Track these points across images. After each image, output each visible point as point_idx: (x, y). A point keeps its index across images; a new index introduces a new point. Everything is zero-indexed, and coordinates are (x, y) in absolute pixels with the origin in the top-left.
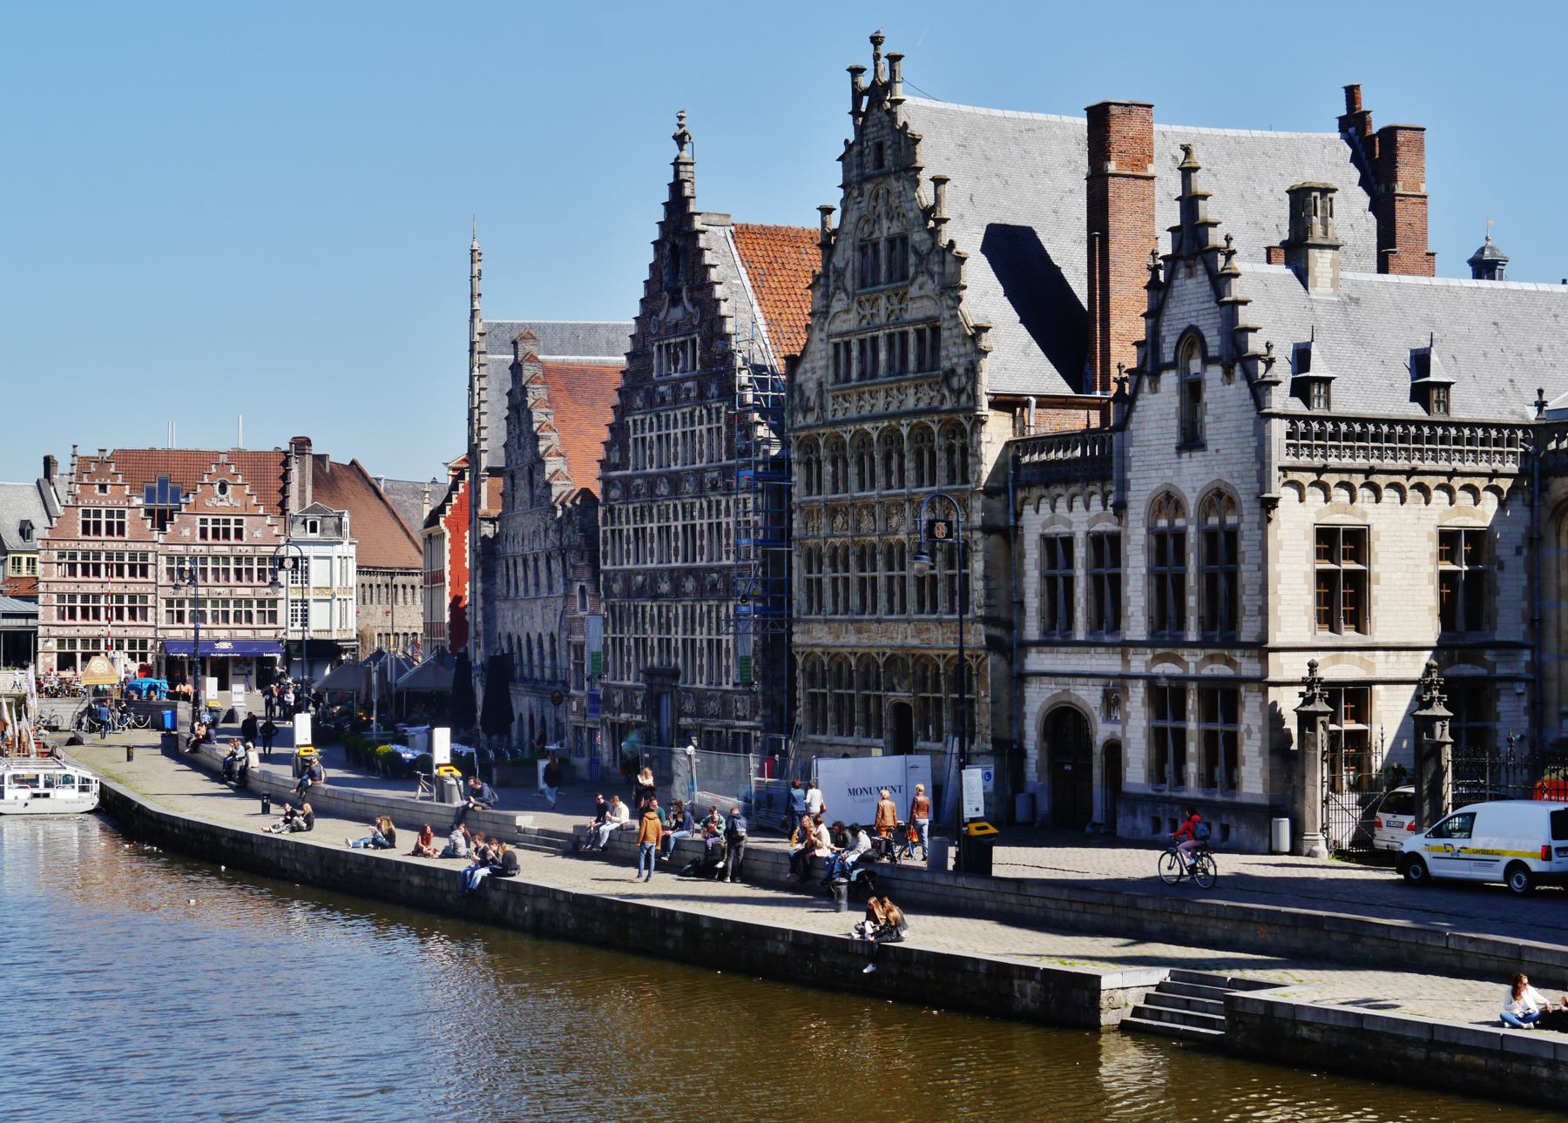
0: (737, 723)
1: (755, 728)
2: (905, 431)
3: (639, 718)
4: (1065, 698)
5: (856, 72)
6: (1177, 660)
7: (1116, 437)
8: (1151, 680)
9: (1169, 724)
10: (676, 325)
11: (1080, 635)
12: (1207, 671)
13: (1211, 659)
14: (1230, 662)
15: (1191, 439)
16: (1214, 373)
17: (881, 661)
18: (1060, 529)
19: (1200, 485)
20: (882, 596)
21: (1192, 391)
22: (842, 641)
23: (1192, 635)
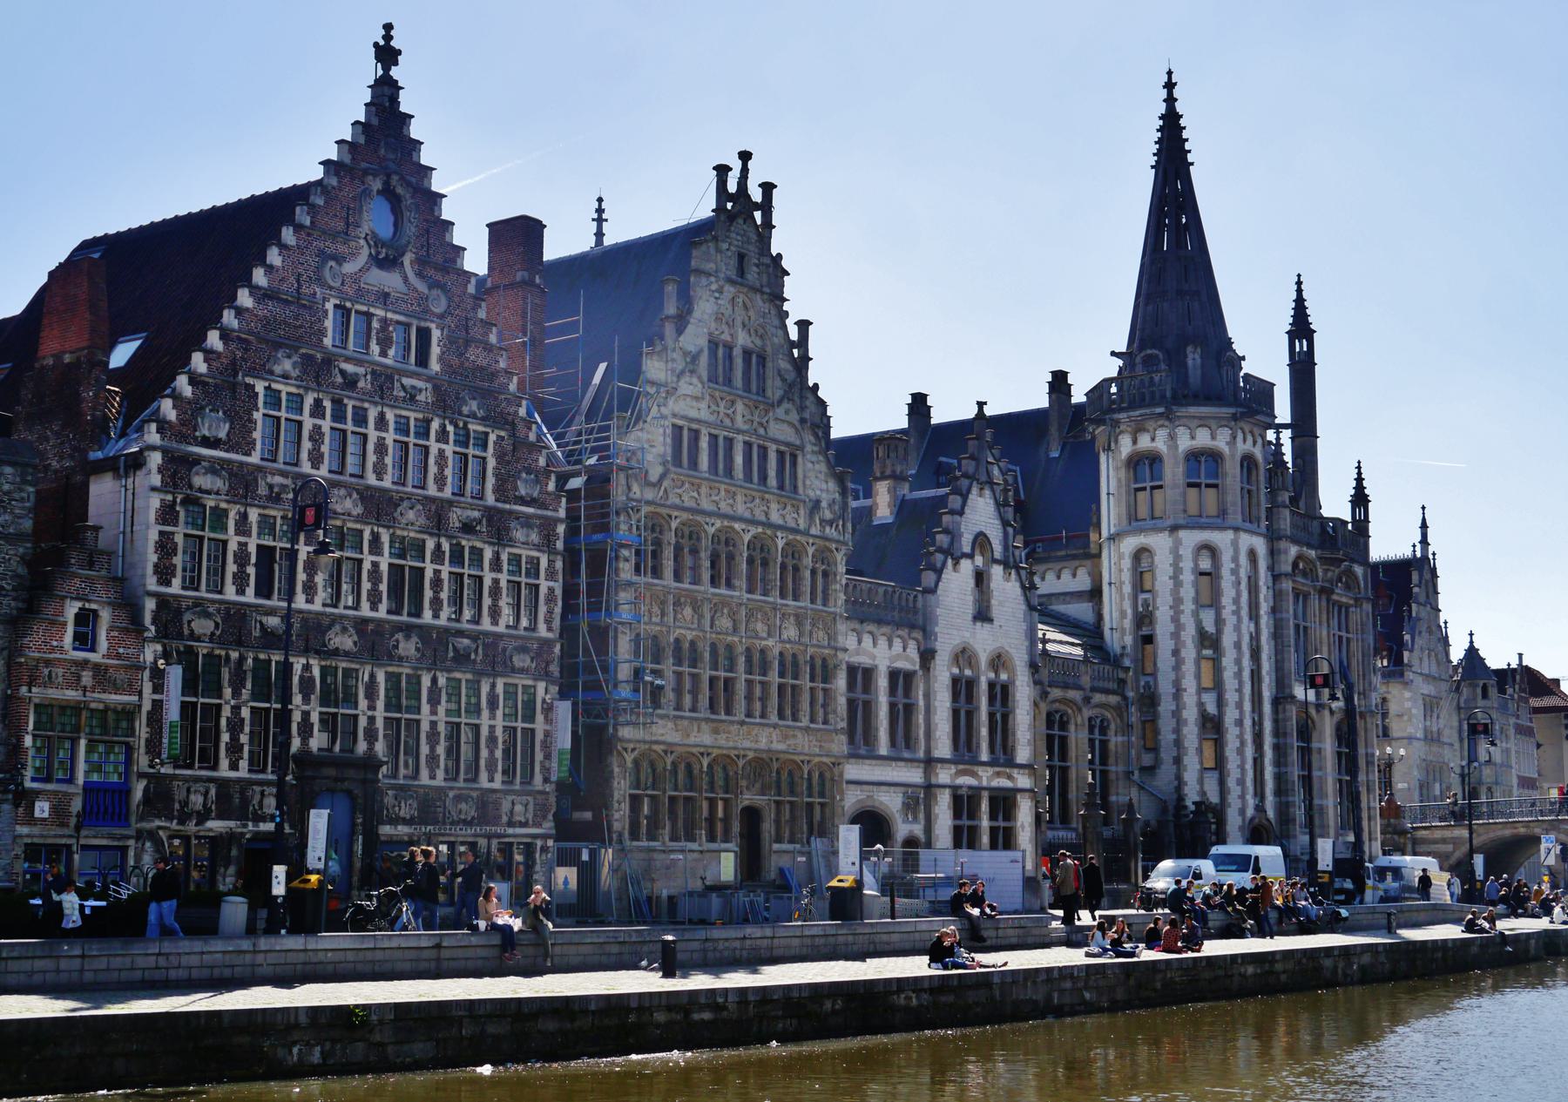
0: (510, 831)
1: (545, 837)
2: (780, 543)
3: (269, 827)
4: (869, 803)
5: (722, 170)
6: (974, 774)
7: (929, 596)
8: (955, 789)
9: (965, 822)
10: (387, 295)
11: (883, 749)
12: (995, 783)
13: (998, 774)
14: (1010, 777)
15: (982, 615)
16: (997, 571)
17: (741, 763)
18: (864, 660)
19: (989, 648)
20: (805, 705)
21: (980, 578)
22: (692, 740)
23: (985, 757)
